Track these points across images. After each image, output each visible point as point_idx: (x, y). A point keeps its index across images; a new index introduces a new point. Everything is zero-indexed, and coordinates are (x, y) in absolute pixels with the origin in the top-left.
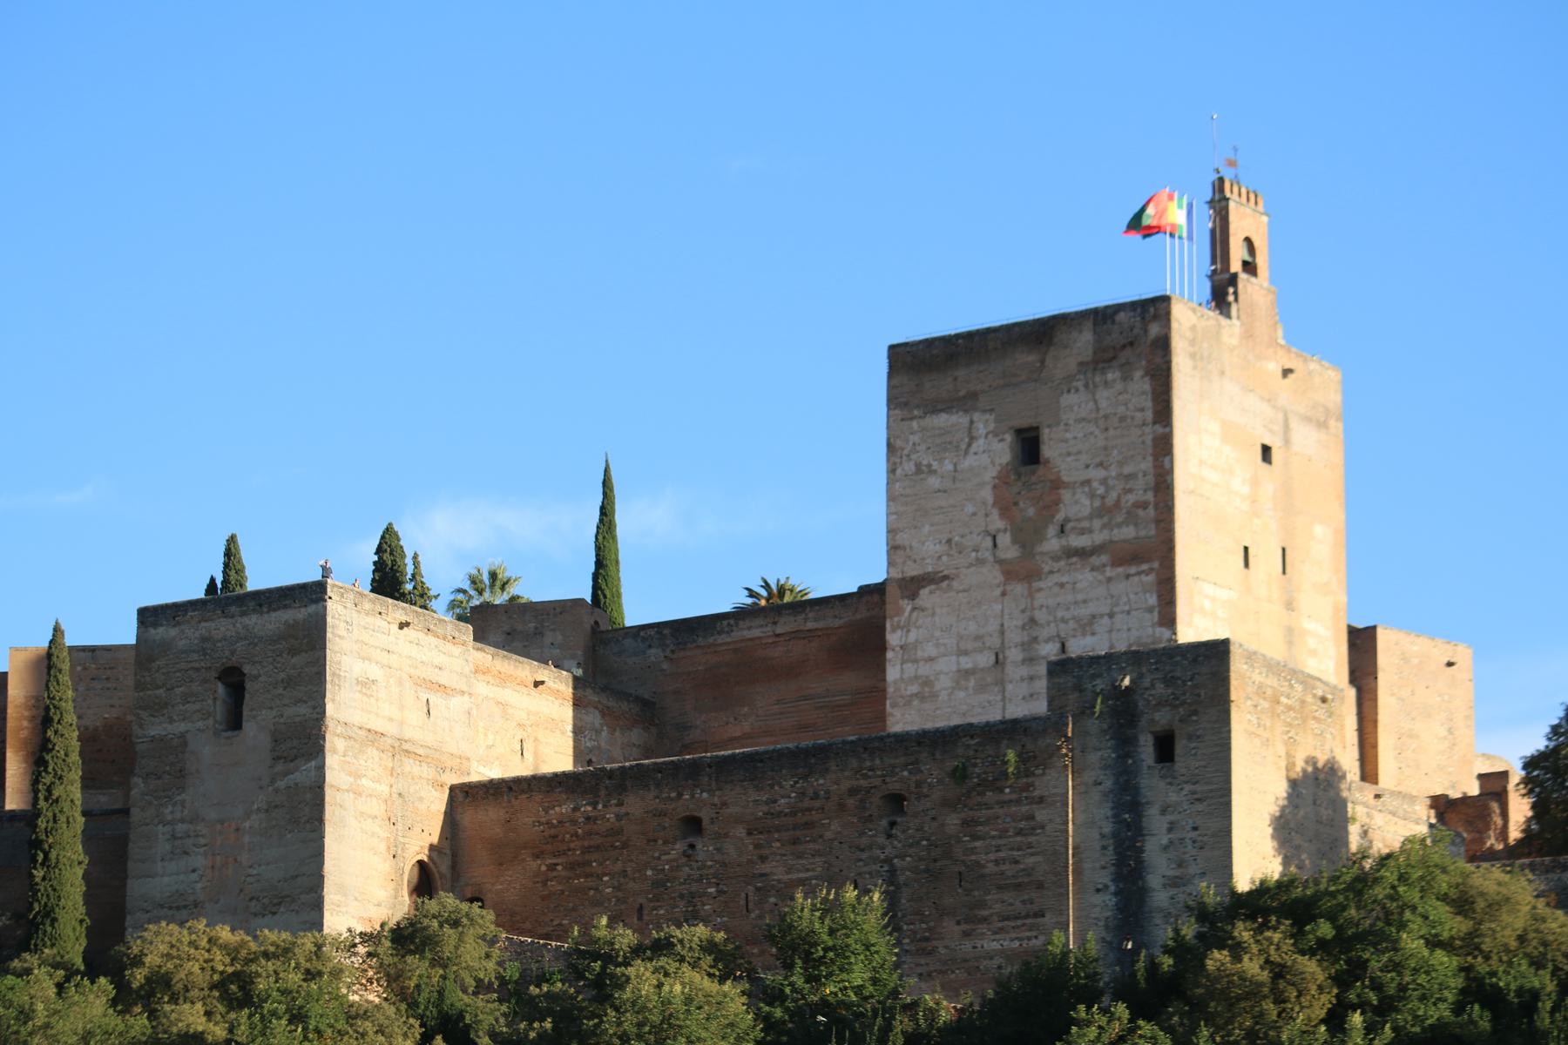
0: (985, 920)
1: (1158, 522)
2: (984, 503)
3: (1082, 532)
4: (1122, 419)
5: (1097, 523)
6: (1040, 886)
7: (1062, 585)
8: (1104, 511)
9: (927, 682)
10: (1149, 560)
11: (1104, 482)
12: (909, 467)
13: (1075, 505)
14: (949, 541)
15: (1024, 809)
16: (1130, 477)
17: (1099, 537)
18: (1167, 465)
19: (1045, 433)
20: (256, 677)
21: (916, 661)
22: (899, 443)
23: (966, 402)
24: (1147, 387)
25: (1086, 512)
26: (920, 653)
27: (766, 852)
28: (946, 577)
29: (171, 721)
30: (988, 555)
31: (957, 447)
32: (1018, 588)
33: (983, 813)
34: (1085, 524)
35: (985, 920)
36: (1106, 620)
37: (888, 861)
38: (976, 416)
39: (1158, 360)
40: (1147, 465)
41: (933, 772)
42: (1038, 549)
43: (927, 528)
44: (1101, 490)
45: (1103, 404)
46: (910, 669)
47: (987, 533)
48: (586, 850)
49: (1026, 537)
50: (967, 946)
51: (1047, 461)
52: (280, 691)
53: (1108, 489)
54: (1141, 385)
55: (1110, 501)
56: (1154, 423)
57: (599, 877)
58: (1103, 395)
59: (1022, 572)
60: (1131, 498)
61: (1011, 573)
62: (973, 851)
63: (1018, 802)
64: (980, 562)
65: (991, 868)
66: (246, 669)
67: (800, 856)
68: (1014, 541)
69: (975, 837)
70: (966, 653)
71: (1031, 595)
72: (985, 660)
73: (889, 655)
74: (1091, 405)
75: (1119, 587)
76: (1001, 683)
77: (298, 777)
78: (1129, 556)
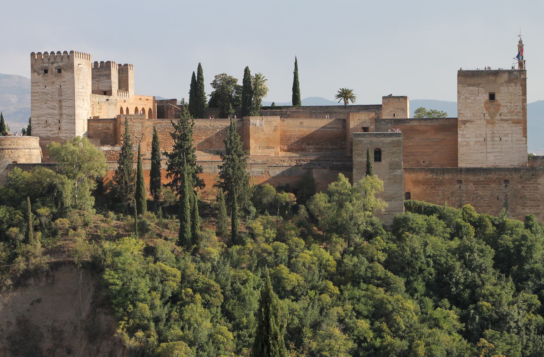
0: (527, 206)
1: (523, 116)
2: (482, 107)
3: (505, 116)
4: (515, 94)
5: (509, 115)
6: (539, 201)
7: (500, 126)
8: (510, 112)
9: (468, 142)
10: (521, 124)
11: (510, 106)
12: (464, 97)
13: (504, 110)
14: (473, 114)
15: (536, 185)
16: (516, 106)
17: (509, 118)
18: (525, 105)
19: (496, 94)
20: (385, 151)
21: (465, 138)
22: (461, 92)
23: (478, 85)
24: (521, 88)
25: (506, 112)
26: (466, 136)
27: (477, 189)
28: (473, 121)
29: (363, 158)
30: (483, 118)
31: (475, 95)
32: (490, 126)
33: (526, 185)
34: (506, 114)
35: (527, 206)
36: (511, 135)
37: (505, 193)
38: (480, 88)
39: (523, 83)
40: (521, 104)
41: (516, 176)
42: (495, 118)
43: (468, 110)
44: (510, 108)
45: (510, 90)
46: (464, 139)
47: (483, 113)
48: (435, 185)
49: (492, 116)
50: (523, 211)
51: (497, 100)
52: (391, 154)
53: (511, 108)
54: (519, 88)
55: (512, 110)
56: (522, 96)
57: (438, 191)
58: (510, 88)
59: (491, 122)
60: (517, 110)
61: (488, 122)
62: (524, 193)
63: (534, 184)
64: (481, 119)
65: (528, 196)
66: (382, 149)
67: (485, 190)
68: (489, 116)
69: (525, 190)
70: (477, 137)
71: (493, 128)
72: (482, 139)
73: (459, 136)
74: (507, 90)
75: (514, 128)
76: (486, 145)
77: (396, 173)
78: (517, 122)
